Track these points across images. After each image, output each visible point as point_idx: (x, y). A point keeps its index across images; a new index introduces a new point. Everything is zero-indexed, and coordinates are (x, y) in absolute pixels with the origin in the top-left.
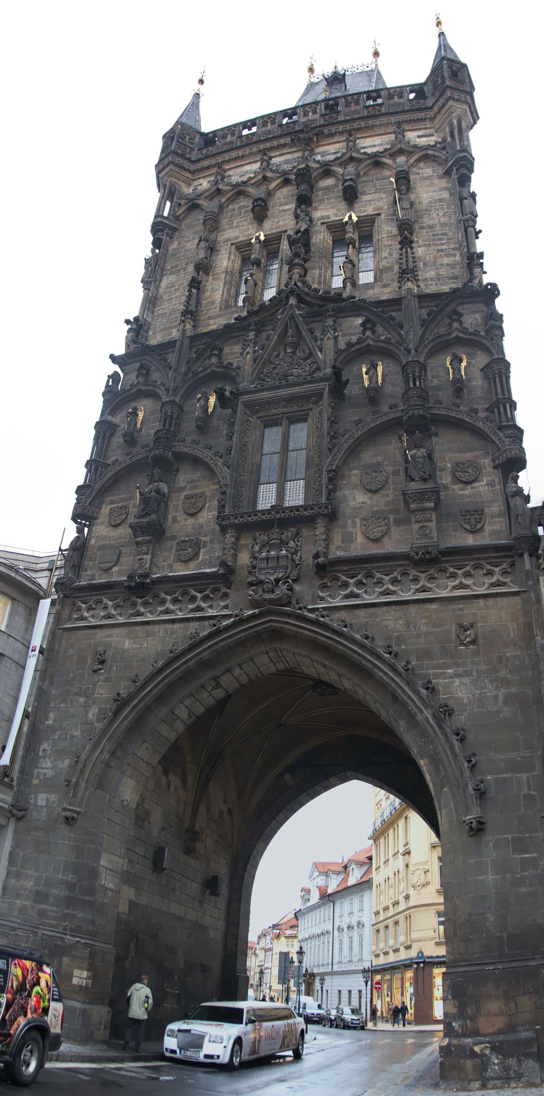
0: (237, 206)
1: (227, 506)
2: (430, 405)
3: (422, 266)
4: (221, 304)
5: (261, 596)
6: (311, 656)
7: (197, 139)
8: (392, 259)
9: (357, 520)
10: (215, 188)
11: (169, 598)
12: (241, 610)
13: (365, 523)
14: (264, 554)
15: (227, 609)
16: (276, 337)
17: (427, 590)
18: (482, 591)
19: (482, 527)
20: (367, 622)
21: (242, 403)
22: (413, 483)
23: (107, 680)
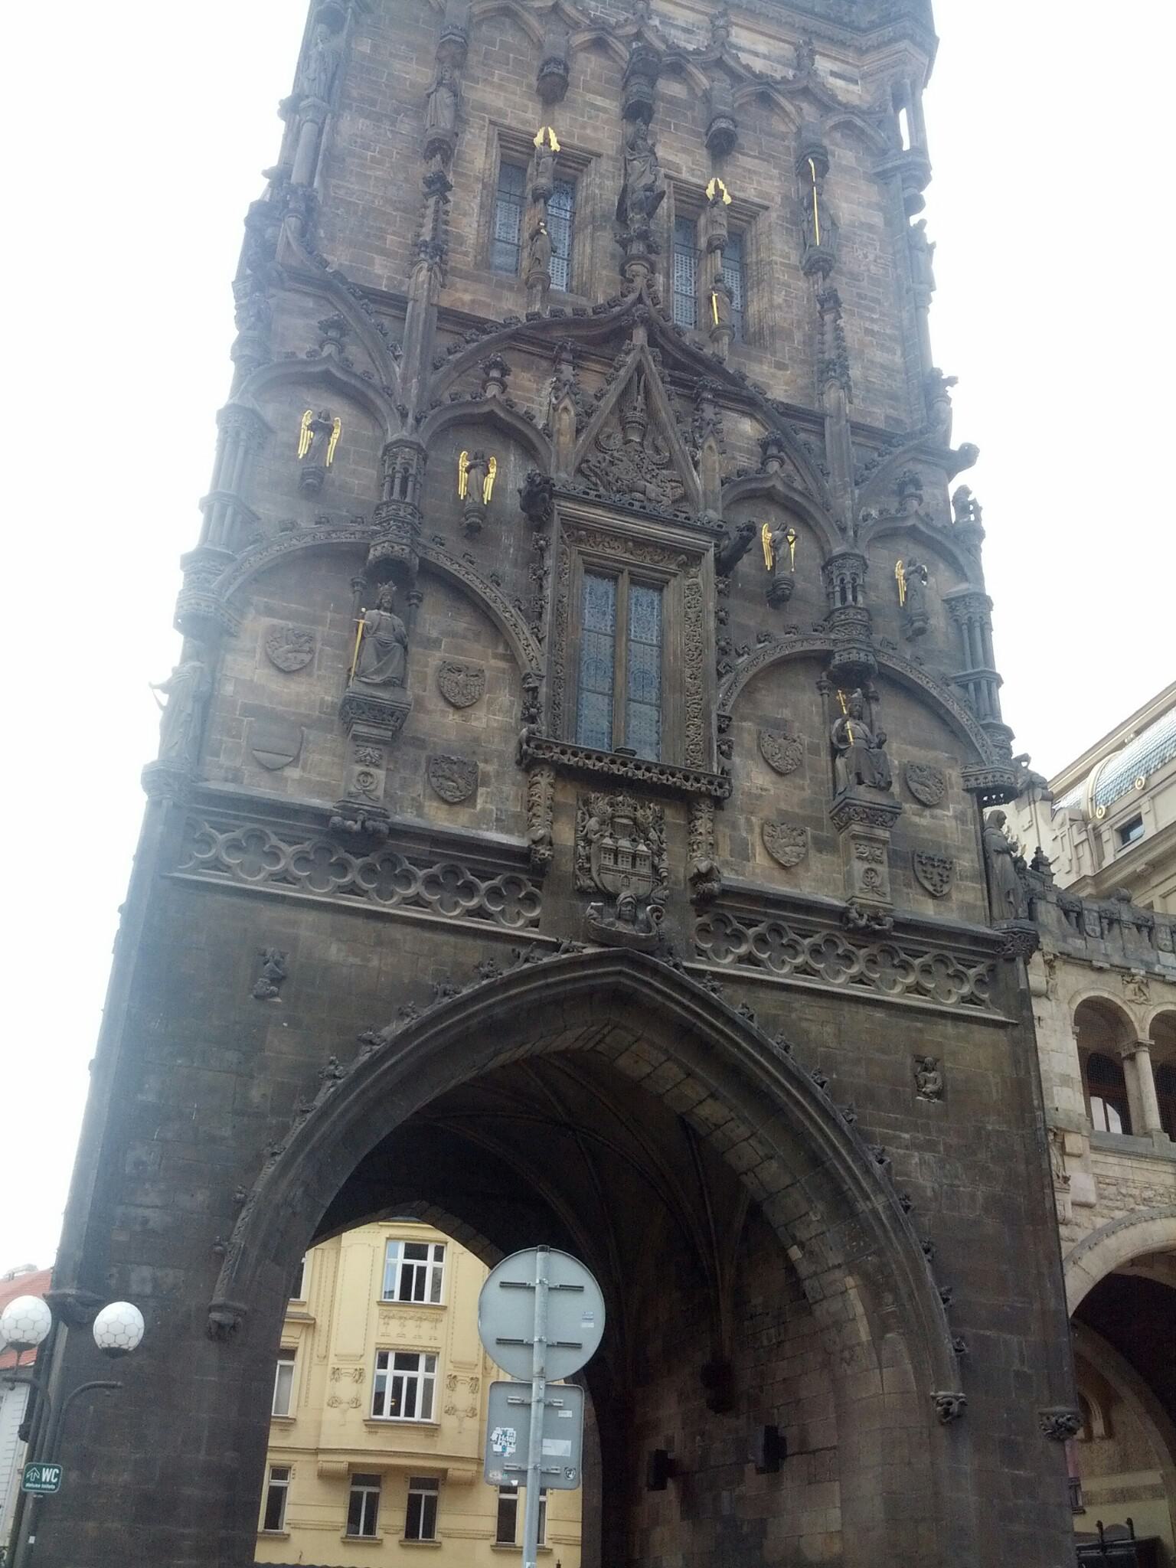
5: (612, 924)
6: (672, 1051)
15: (537, 927)
17: (865, 980)
18: (950, 1004)
22: (862, 788)
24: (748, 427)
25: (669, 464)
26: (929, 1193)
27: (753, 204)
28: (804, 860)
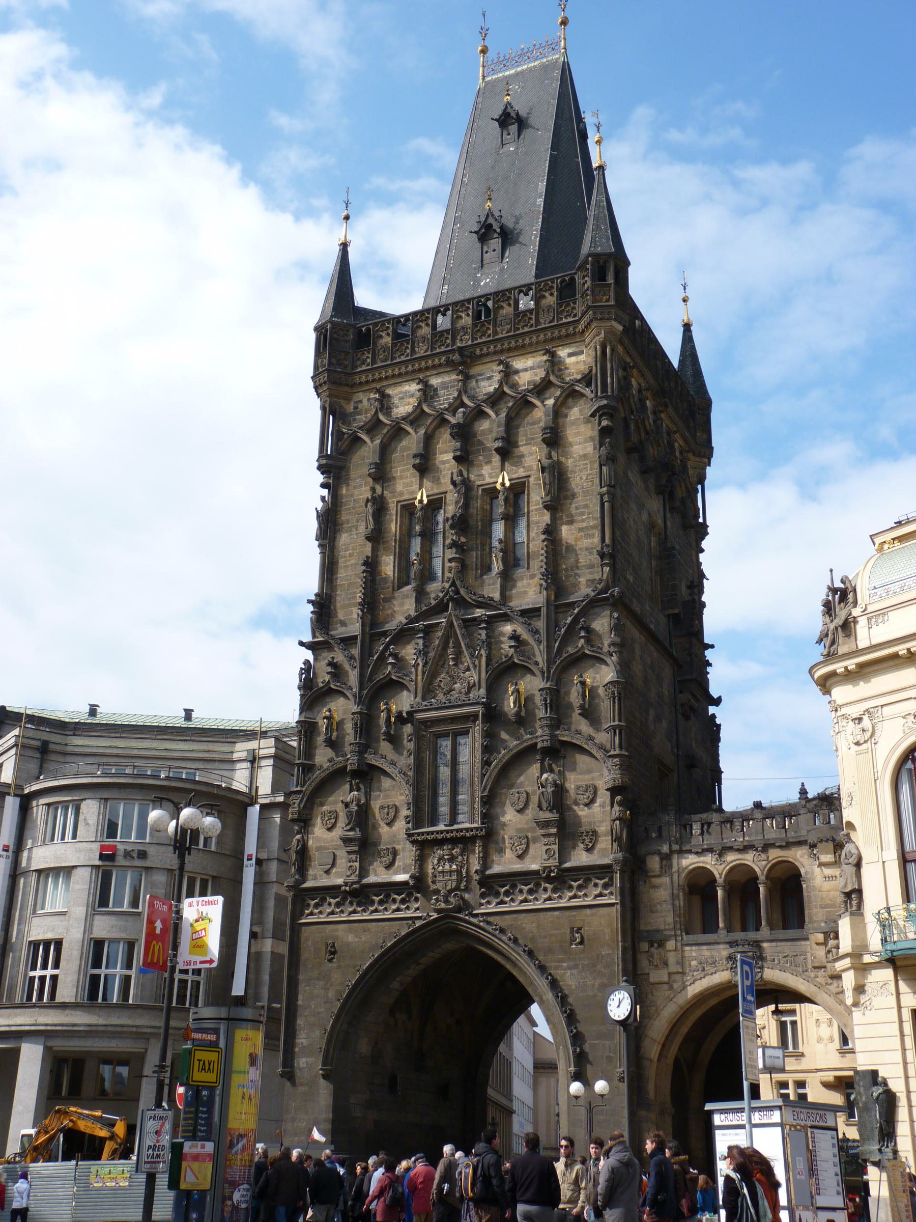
12: (428, 914)
13: (511, 841)
14: (441, 868)
18: (589, 901)
20: (512, 925)
22: (541, 812)
23: (339, 967)
24: (508, 628)
25: (468, 669)
26: (574, 987)
28: (526, 851)
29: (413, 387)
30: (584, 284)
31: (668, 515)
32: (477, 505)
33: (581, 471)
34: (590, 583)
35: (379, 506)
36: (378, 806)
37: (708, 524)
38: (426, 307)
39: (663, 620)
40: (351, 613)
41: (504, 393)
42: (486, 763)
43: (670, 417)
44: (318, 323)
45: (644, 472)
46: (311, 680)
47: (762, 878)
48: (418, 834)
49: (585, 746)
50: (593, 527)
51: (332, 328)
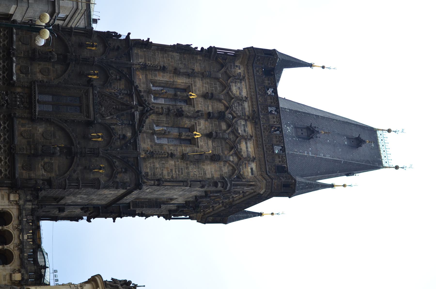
0: (217, 86)
1: (40, 83)
2: (78, 156)
3: (162, 162)
4: (154, 80)
7: (272, 66)
8: (167, 150)
9: (31, 128)
10: (232, 76)
11: (5, 64)
14: (18, 96)
16: (122, 101)
19: (24, 170)
21: (89, 88)
22: (41, 146)
24: (129, 134)
27: (198, 144)
28: (24, 137)
29: (244, 93)
30: (283, 177)
31: (176, 205)
32: (187, 123)
33: (199, 171)
34: (147, 174)
35: (191, 75)
36: (50, 67)
37: (171, 220)
38: (279, 99)
39: (128, 201)
40: (142, 59)
41: (237, 137)
42: (66, 121)
43: (220, 208)
44: (277, 51)
45: (196, 197)
46: (111, 38)
47: (6, 247)
48: (35, 87)
49: (71, 168)
50: (173, 175)
51: (274, 59)
